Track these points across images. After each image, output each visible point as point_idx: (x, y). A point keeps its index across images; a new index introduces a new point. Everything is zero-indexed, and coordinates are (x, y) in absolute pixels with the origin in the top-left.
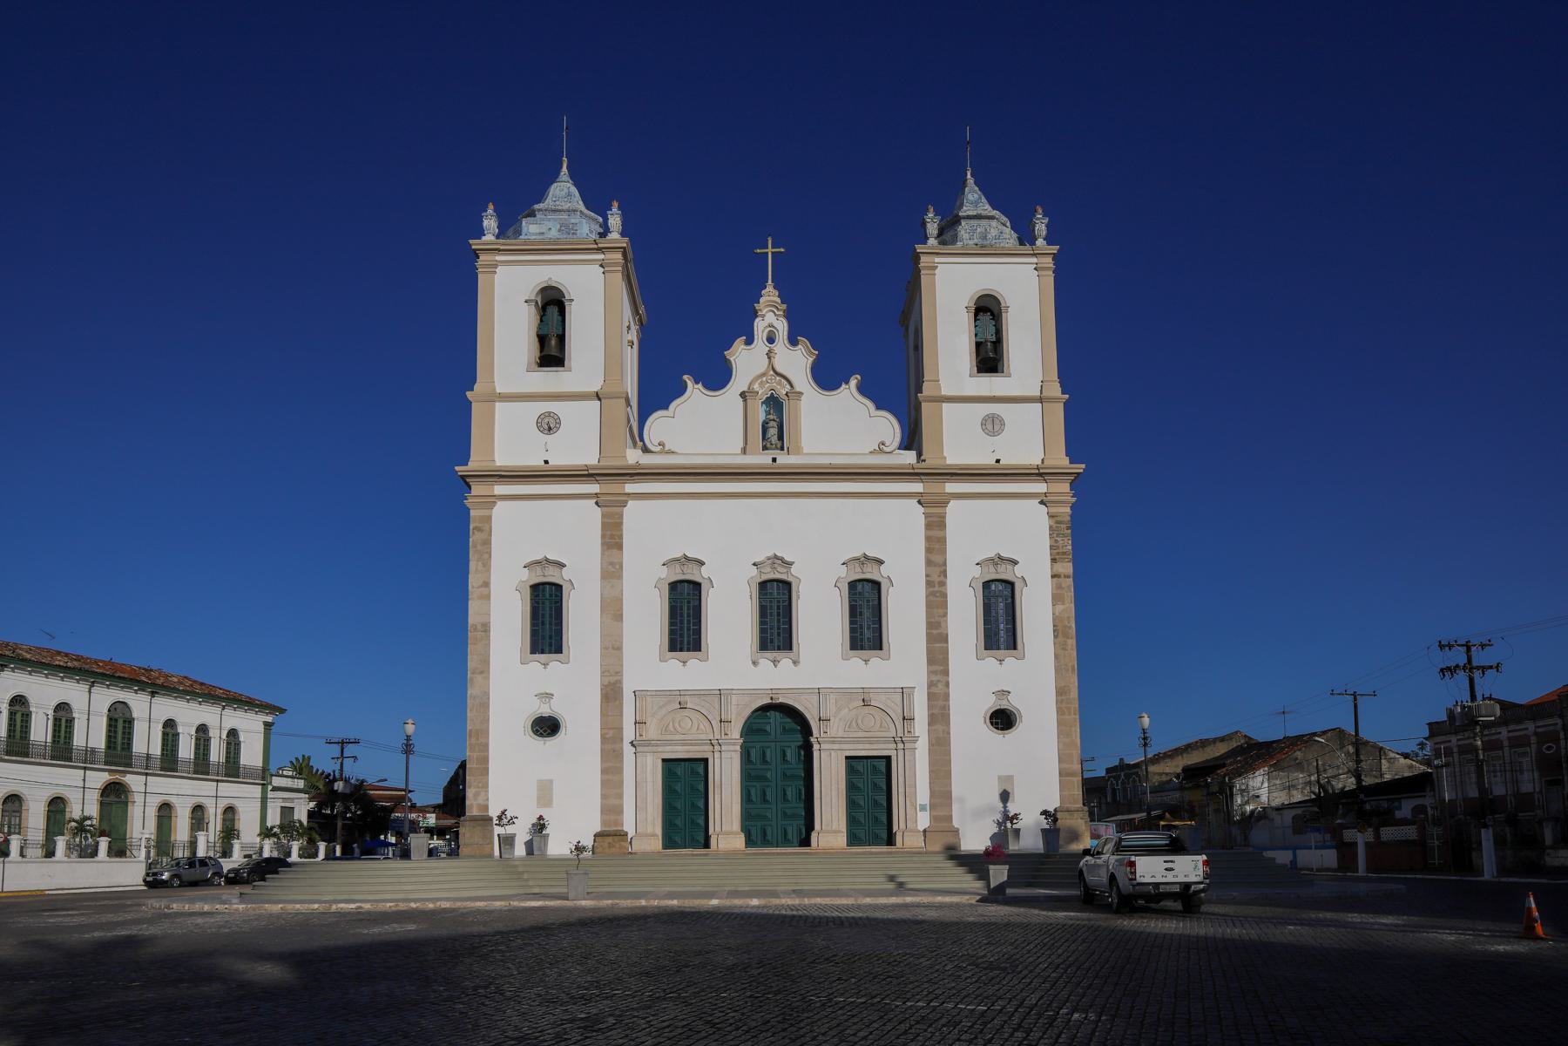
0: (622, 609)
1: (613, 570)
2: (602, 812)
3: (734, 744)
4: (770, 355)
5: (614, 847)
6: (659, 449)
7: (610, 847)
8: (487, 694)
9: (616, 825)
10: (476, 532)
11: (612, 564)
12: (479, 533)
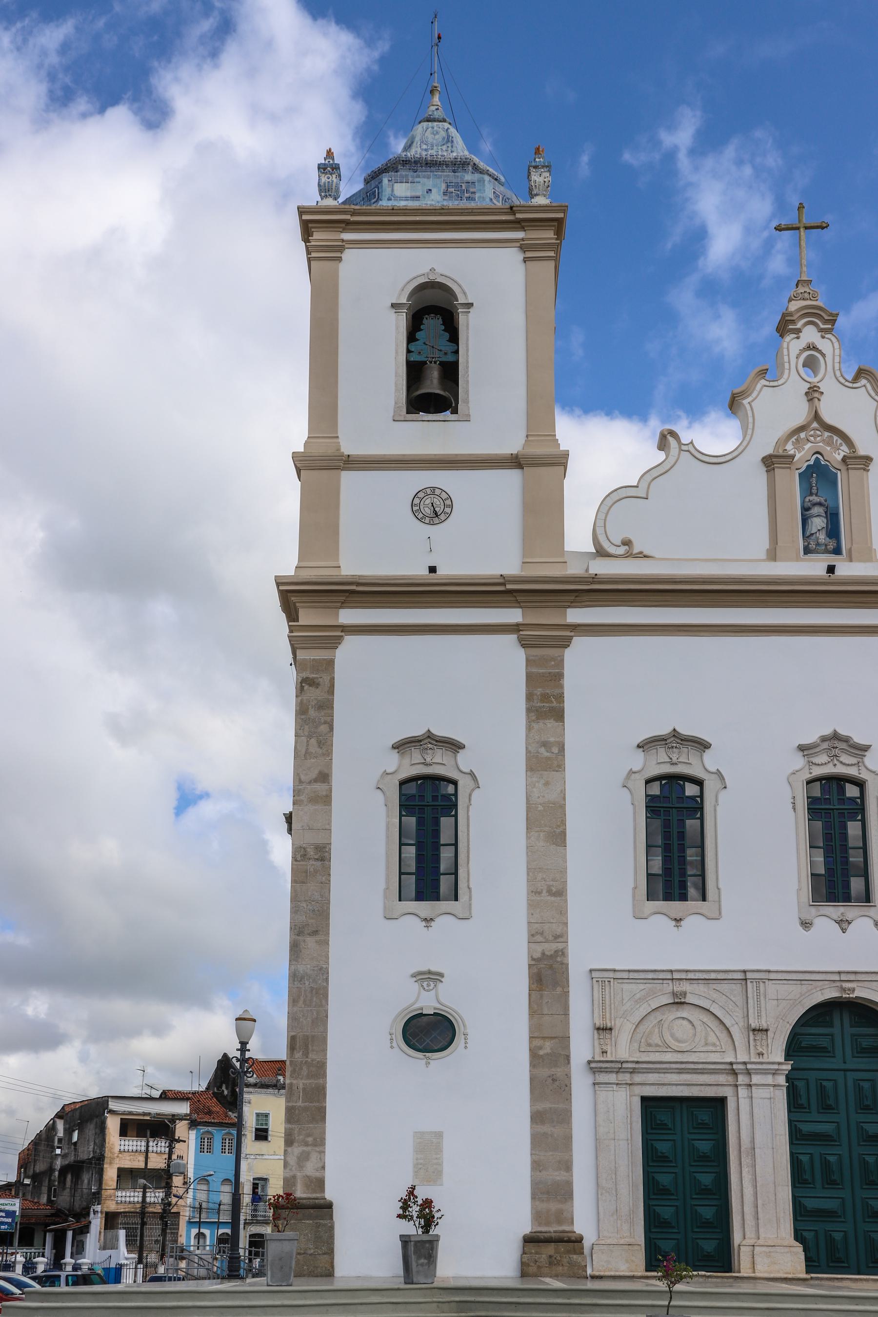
0: (563, 822)
1: (548, 754)
2: (534, 1197)
3: (775, 1073)
4: (813, 394)
5: (559, 1263)
6: (622, 550)
7: (551, 1264)
8: (324, 972)
9: (560, 1222)
10: (306, 687)
11: (545, 744)
12: (312, 689)
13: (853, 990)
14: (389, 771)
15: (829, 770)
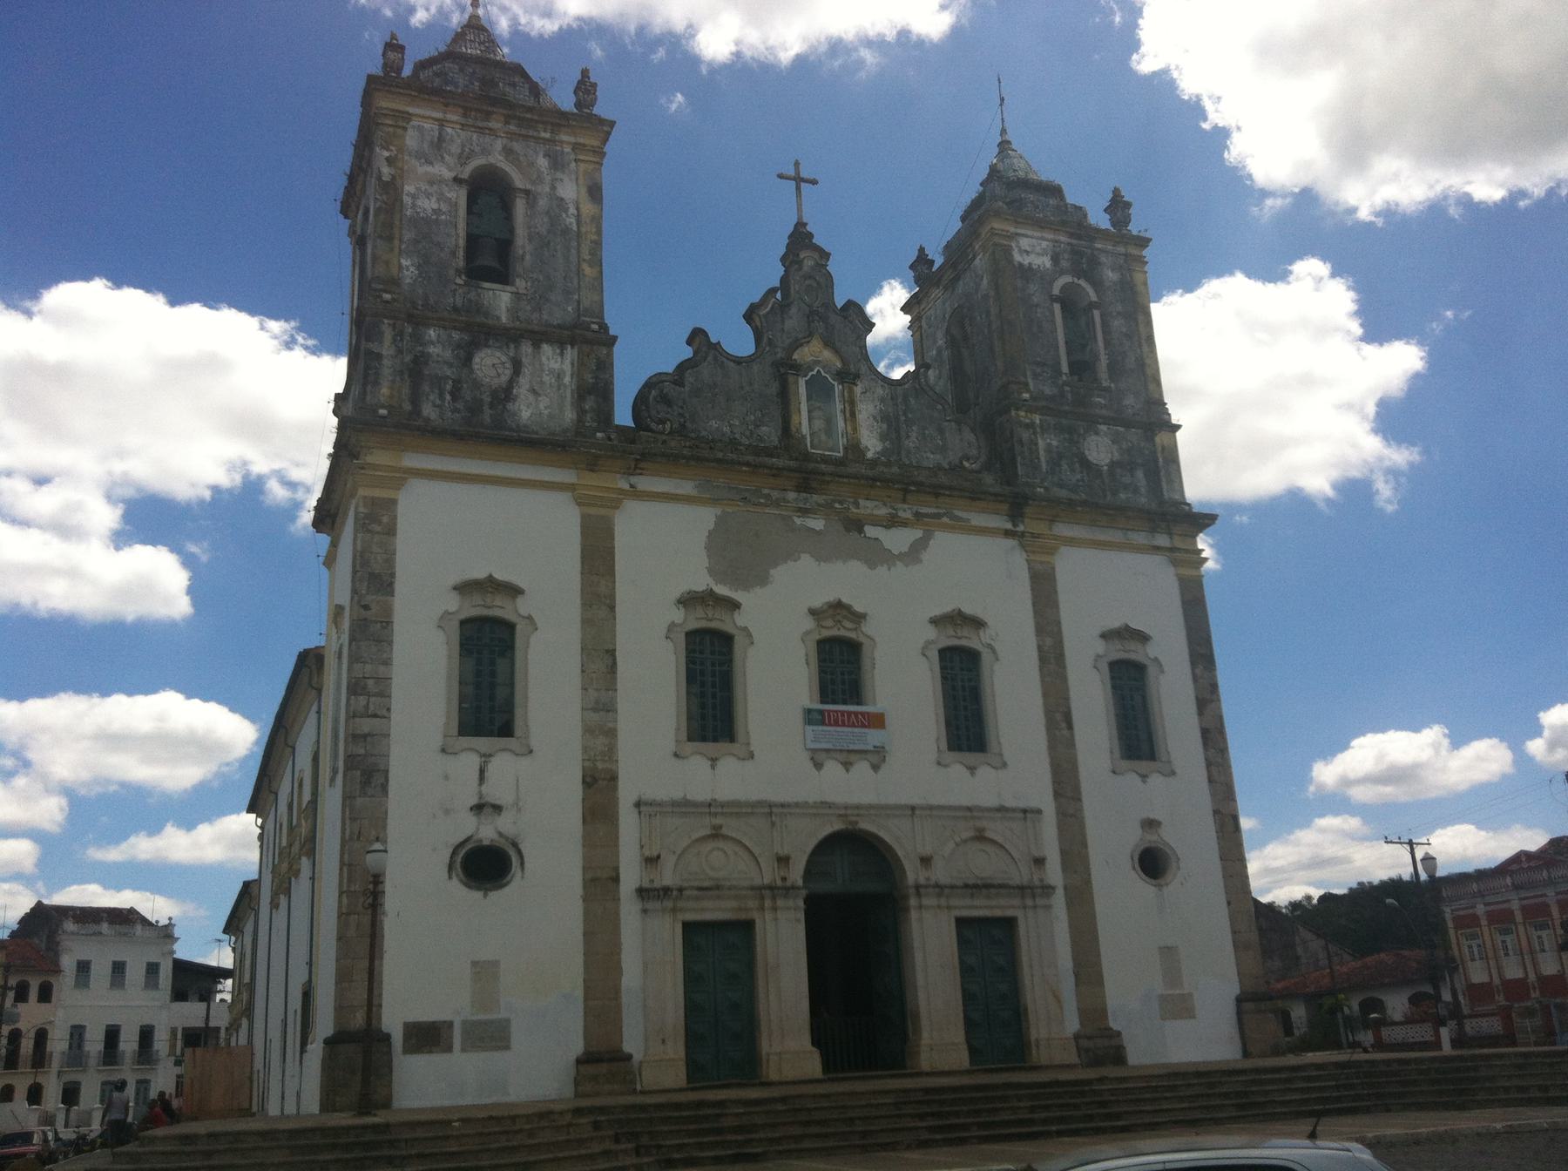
13: (857, 823)
14: (450, 611)
15: (834, 632)
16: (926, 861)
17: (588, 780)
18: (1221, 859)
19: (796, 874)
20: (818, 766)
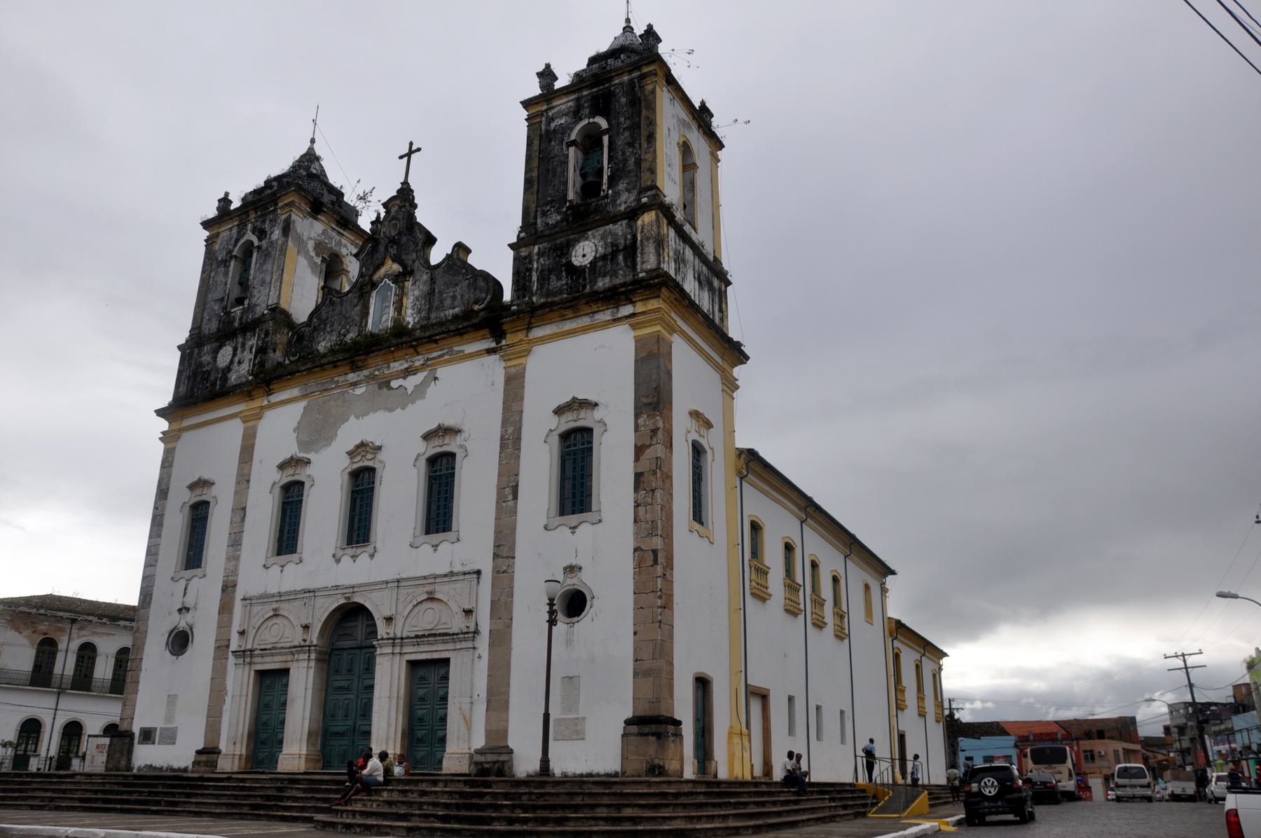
16: (389, 620)
17: (224, 588)
18: (635, 593)
19: (314, 637)
20: (338, 561)
